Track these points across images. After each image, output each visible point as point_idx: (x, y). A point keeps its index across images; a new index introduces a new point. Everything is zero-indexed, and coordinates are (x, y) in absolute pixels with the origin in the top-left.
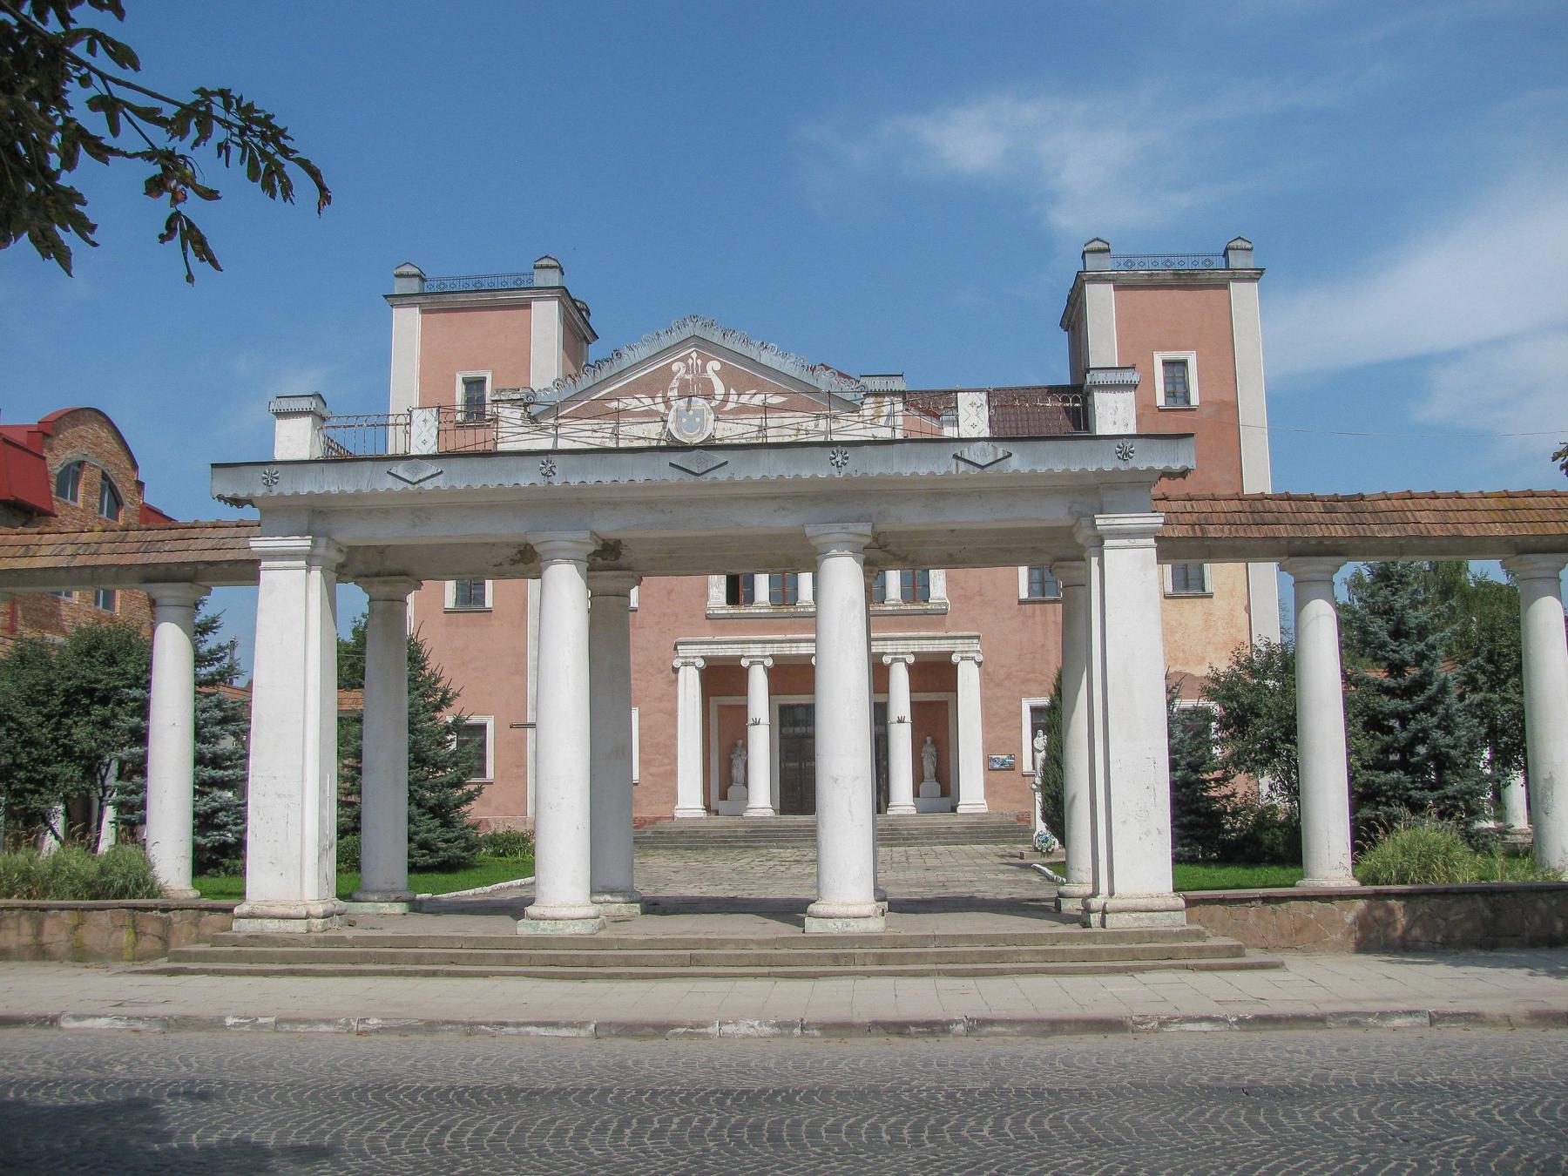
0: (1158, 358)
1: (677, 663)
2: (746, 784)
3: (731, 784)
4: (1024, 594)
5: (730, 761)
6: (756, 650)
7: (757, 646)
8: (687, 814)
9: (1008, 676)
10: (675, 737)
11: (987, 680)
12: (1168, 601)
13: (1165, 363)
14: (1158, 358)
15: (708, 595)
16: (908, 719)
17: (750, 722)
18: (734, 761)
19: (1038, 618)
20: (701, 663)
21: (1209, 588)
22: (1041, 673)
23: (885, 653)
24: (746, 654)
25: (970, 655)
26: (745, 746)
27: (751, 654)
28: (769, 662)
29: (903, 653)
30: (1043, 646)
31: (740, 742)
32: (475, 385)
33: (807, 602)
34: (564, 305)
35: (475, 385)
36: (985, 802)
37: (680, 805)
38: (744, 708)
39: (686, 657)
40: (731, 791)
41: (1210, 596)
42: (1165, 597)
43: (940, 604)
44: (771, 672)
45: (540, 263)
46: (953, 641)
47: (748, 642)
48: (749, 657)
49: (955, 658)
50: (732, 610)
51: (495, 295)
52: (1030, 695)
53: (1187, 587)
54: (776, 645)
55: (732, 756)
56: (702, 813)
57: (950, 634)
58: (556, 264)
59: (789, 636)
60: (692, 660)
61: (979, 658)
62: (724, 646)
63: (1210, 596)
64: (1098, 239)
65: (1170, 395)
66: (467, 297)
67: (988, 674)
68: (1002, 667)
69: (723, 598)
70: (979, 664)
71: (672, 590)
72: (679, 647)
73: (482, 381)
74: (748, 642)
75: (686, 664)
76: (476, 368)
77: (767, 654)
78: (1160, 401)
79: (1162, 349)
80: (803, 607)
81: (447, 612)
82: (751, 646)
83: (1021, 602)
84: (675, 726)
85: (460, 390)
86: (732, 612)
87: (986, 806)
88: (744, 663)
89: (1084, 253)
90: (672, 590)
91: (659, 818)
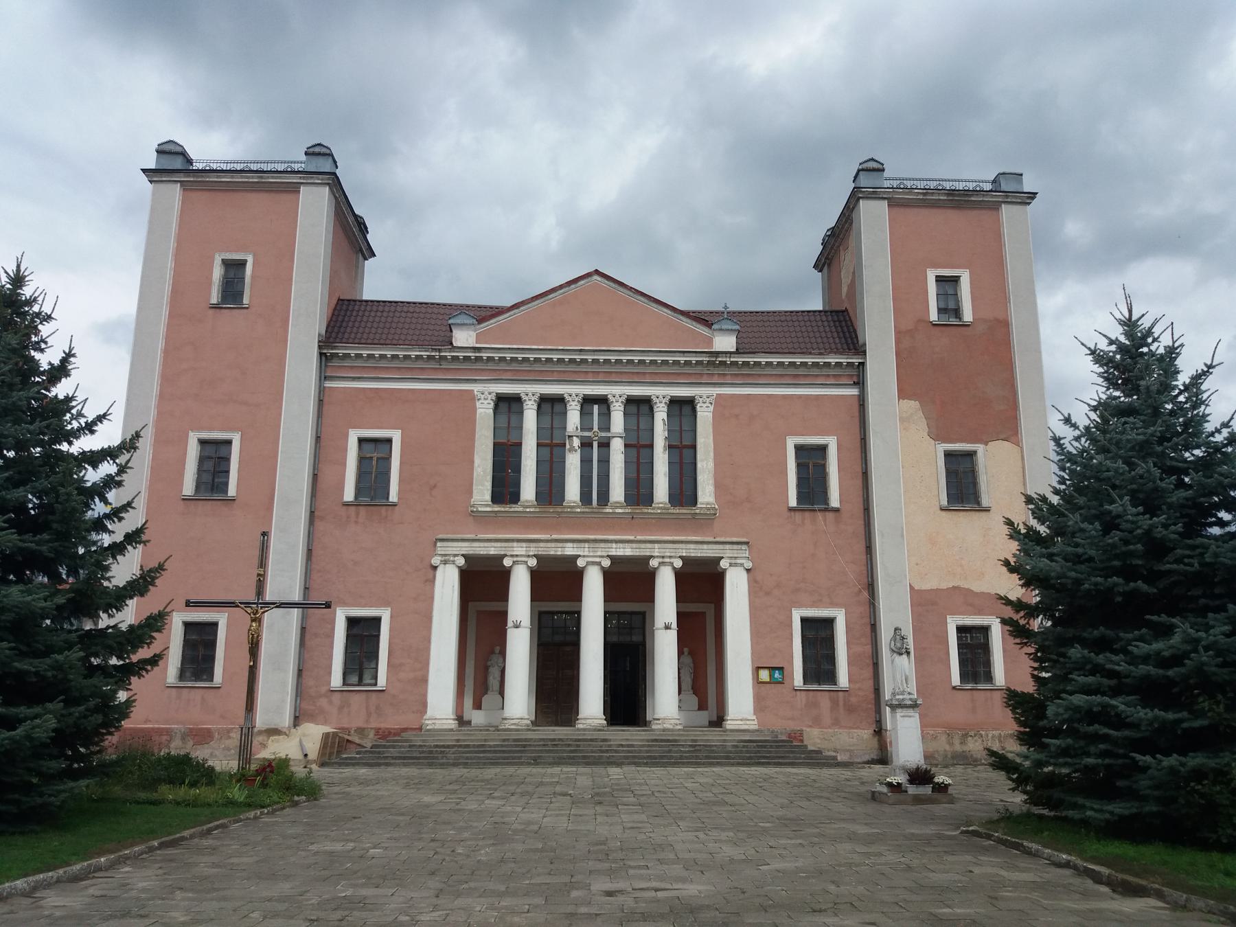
0: (931, 276)
1: (436, 561)
2: (502, 692)
3: (486, 694)
4: (793, 502)
5: (486, 668)
6: (519, 549)
7: (520, 544)
8: (439, 725)
10: (428, 640)
11: (756, 588)
12: (944, 513)
13: (939, 279)
14: (931, 276)
16: (674, 625)
17: (510, 624)
18: (491, 670)
20: (461, 561)
21: (985, 502)
23: (652, 557)
24: (509, 553)
25: (739, 561)
26: (503, 653)
27: (515, 553)
28: (533, 562)
29: (670, 557)
31: (497, 649)
32: (234, 268)
34: (335, 197)
35: (234, 268)
36: (754, 718)
37: (430, 713)
38: (504, 615)
39: (446, 555)
40: (485, 700)
41: (987, 510)
42: (941, 509)
43: (708, 509)
44: (535, 575)
45: (311, 150)
46: (721, 547)
47: (512, 540)
48: (512, 556)
49: (724, 564)
50: (497, 508)
51: (261, 177)
52: (800, 605)
54: (542, 545)
55: (489, 663)
56: (452, 724)
57: (718, 539)
58: (328, 152)
59: (555, 536)
60: (452, 558)
61: (749, 565)
62: (486, 544)
63: (987, 510)
64: (872, 160)
65: (941, 311)
66: (232, 177)
67: (756, 582)
68: (771, 575)
69: (488, 497)
70: (748, 571)
71: (435, 486)
72: (439, 544)
73: (242, 264)
74: (512, 540)
75: (445, 562)
76: (237, 251)
77: (531, 553)
78: (933, 316)
79: (935, 266)
80: (569, 507)
81: (186, 500)
82: (515, 544)
83: (791, 509)
85: (217, 272)
86: (496, 509)
87: (756, 723)
88: (507, 562)
89: (859, 171)
90: (435, 486)
91: (405, 730)
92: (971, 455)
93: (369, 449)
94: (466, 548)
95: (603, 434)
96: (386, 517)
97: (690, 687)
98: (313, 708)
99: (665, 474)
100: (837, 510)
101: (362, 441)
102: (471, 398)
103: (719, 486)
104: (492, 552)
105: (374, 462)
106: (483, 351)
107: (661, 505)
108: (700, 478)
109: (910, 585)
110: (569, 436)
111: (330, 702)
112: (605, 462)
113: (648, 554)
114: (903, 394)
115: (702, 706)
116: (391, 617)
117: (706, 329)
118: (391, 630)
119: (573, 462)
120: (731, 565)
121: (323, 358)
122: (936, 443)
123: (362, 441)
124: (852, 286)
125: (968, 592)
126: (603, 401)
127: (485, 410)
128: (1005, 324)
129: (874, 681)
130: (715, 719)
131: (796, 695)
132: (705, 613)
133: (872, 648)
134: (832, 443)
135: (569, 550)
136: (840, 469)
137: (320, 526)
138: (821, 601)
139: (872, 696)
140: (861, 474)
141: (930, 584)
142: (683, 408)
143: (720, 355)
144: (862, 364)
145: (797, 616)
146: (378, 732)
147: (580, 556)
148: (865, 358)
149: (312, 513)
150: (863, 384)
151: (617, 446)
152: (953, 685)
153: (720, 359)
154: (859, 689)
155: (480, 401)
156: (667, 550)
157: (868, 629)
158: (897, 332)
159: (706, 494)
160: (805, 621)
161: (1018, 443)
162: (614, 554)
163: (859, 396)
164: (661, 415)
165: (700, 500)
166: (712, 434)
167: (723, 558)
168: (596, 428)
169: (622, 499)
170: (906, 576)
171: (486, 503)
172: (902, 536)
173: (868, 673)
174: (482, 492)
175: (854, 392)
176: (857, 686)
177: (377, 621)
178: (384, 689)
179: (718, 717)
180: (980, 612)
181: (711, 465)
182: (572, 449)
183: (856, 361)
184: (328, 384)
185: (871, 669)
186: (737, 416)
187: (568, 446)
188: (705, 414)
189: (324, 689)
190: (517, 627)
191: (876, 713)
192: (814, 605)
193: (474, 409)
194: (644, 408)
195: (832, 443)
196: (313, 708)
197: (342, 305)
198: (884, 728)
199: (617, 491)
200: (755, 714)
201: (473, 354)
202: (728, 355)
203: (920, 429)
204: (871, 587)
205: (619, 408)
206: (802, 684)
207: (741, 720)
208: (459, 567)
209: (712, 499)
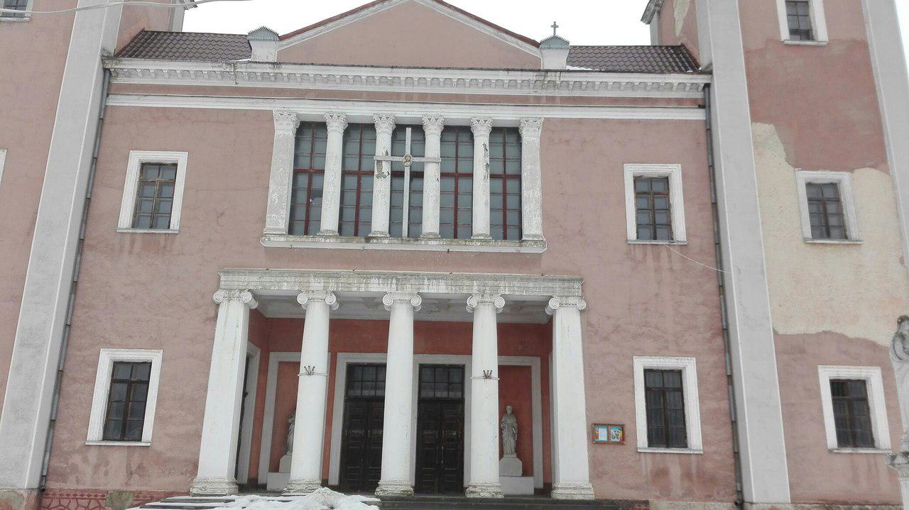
6: (316, 284)
9: (617, 329)
11: (590, 332)
15: (264, 222)
16: (495, 374)
17: (302, 370)
19: (650, 263)
22: (657, 328)
30: (657, 295)
33: (382, 233)
41: (857, 244)
52: (643, 353)
53: (828, 236)
61: (583, 305)
65: (794, 32)
67: (591, 325)
68: (609, 317)
69: (283, 224)
70: (582, 312)
71: (222, 214)
78: (785, 34)
84: (207, 374)
90: (222, 214)
92: (834, 186)
93: (152, 174)
94: (254, 281)
95: (417, 160)
96: (165, 247)
97: (513, 450)
98: (65, 466)
99: (486, 204)
100: (683, 247)
101: (144, 166)
102: (268, 117)
103: (546, 216)
104: (285, 287)
105: (156, 188)
106: (283, 66)
107: (480, 238)
108: (526, 209)
109: (774, 330)
110: (378, 161)
111: (85, 460)
112: (417, 192)
113: (465, 292)
114: (756, 117)
115: (527, 471)
116: (163, 360)
117: (534, 48)
118: (162, 375)
119: (381, 188)
120: (561, 305)
121: (108, 75)
122: (796, 169)
123: (144, 166)
124: (691, 19)
125: (841, 338)
126: (419, 129)
127: (285, 132)
128: (863, 46)
129: (734, 443)
130: (541, 486)
131: (640, 460)
132: (530, 367)
133: (730, 404)
134: (675, 172)
135: (375, 287)
136: (686, 200)
137: (89, 255)
138: (667, 348)
139: (732, 461)
140: (710, 205)
141: (797, 328)
142: (507, 135)
143: (549, 74)
144: (707, 86)
145: (640, 364)
146: (138, 497)
147: (386, 293)
148: (712, 79)
149: (81, 241)
150: (709, 106)
151: (432, 174)
152: (829, 448)
153: (549, 79)
154: (715, 452)
155: (279, 122)
156: (488, 288)
157: (724, 381)
158: (747, 52)
159: (533, 224)
160: (648, 372)
161: (887, 171)
162: (426, 291)
163: (706, 121)
164: (482, 138)
165: (525, 232)
166: (539, 160)
167: (551, 297)
168: (408, 151)
169: (436, 230)
170: (768, 319)
171: (280, 233)
172: (762, 272)
173: (726, 432)
174: (278, 218)
175: (699, 115)
176: (713, 448)
177: (148, 365)
178: (149, 444)
179: (544, 484)
180: (856, 361)
181: (538, 194)
182: (381, 175)
183: (701, 80)
184: (113, 101)
185: (729, 428)
186: (567, 142)
187: (376, 173)
188: (531, 138)
189: (79, 444)
190: (310, 374)
191: (737, 482)
192: (657, 353)
193: (272, 131)
194: (464, 137)
195: (675, 172)
196: (65, 466)
197: (144, 35)
198: (747, 498)
199: (431, 220)
200: (590, 481)
201: (272, 71)
202: (558, 74)
203: (776, 153)
204: (725, 332)
205: (434, 132)
206: (646, 445)
207: (574, 488)
208: (245, 304)
209: (539, 232)
